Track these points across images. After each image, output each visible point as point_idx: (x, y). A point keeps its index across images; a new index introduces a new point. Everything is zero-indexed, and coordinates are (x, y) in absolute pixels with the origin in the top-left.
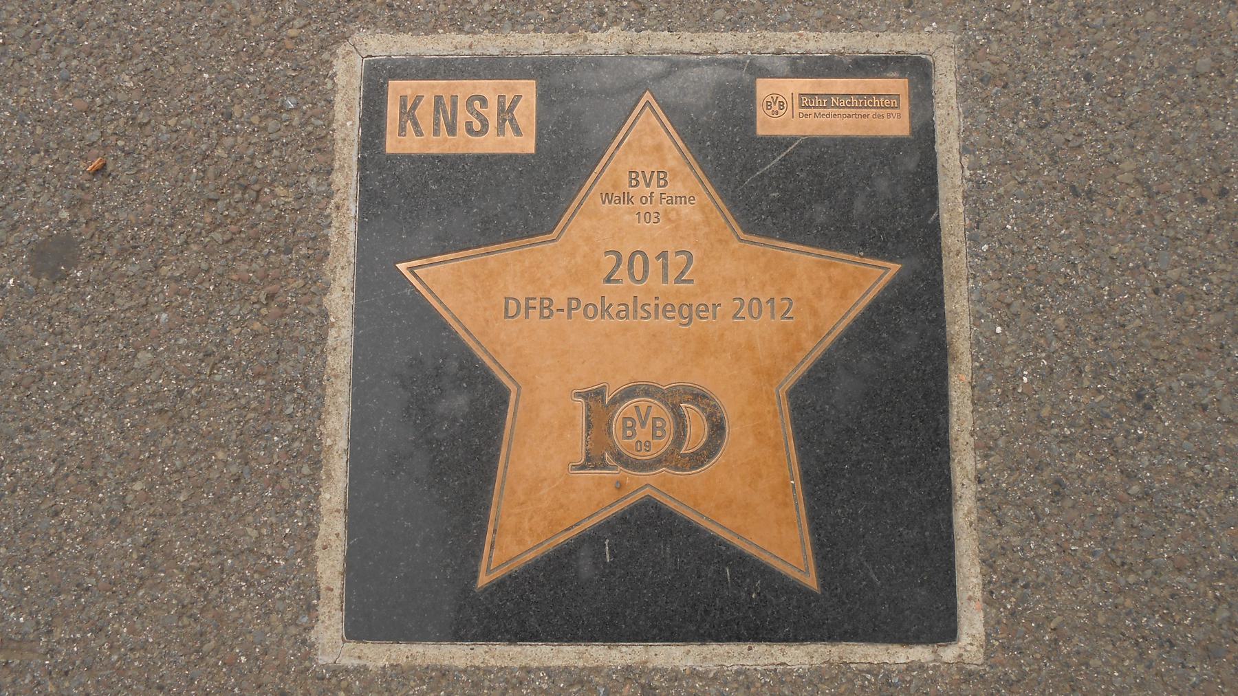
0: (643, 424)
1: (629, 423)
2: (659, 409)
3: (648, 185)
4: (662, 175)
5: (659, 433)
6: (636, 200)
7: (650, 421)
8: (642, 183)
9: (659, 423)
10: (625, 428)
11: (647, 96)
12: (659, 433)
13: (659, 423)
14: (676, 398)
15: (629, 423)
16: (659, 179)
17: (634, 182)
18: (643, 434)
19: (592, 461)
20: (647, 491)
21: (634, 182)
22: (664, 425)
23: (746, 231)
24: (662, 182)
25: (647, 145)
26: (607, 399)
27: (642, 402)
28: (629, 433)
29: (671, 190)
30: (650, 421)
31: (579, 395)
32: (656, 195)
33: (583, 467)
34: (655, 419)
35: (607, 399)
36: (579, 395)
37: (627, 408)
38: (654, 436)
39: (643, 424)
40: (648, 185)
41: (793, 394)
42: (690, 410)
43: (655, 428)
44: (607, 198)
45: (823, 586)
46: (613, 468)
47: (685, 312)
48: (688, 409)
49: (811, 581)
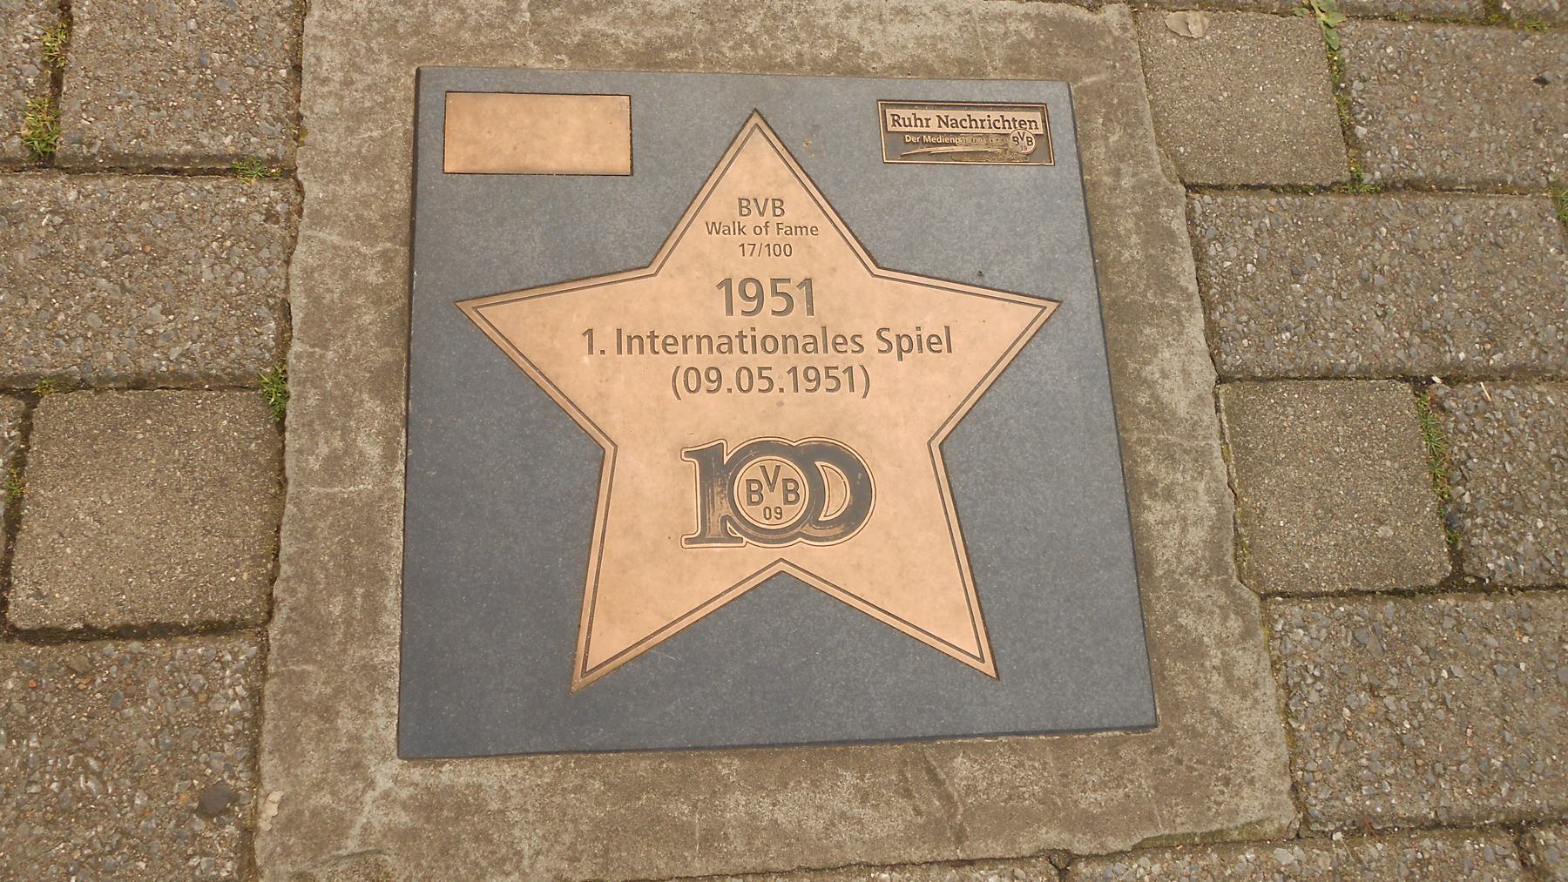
0: (772, 490)
1: (755, 487)
2: (791, 470)
3: (762, 214)
4: (778, 204)
5: (792, 497)
6: (749, 230)
7: (779, 480)
8: (755, 211)
9: (791, 486)
10: (750, 492)
12: (792, 497)
13: (791, 486)
14: (808, 455)
15: (755, 487)
17: (745, 211)
18: (774, 498)
20: (781, 566)
21: (745, 211)
24: (778, 212)
26: (726, 460)
27: (771, 461)
28: (755, 498)
29: (790, 218)
32: (772, 229)
33: (701, 539)
34: (786, 481)
35: (726, 460)
37: (751, 470)
38: (787, 502)
39: (772, 486)
40: (762, 214)
43: (787, 491)
44: (713, 228)
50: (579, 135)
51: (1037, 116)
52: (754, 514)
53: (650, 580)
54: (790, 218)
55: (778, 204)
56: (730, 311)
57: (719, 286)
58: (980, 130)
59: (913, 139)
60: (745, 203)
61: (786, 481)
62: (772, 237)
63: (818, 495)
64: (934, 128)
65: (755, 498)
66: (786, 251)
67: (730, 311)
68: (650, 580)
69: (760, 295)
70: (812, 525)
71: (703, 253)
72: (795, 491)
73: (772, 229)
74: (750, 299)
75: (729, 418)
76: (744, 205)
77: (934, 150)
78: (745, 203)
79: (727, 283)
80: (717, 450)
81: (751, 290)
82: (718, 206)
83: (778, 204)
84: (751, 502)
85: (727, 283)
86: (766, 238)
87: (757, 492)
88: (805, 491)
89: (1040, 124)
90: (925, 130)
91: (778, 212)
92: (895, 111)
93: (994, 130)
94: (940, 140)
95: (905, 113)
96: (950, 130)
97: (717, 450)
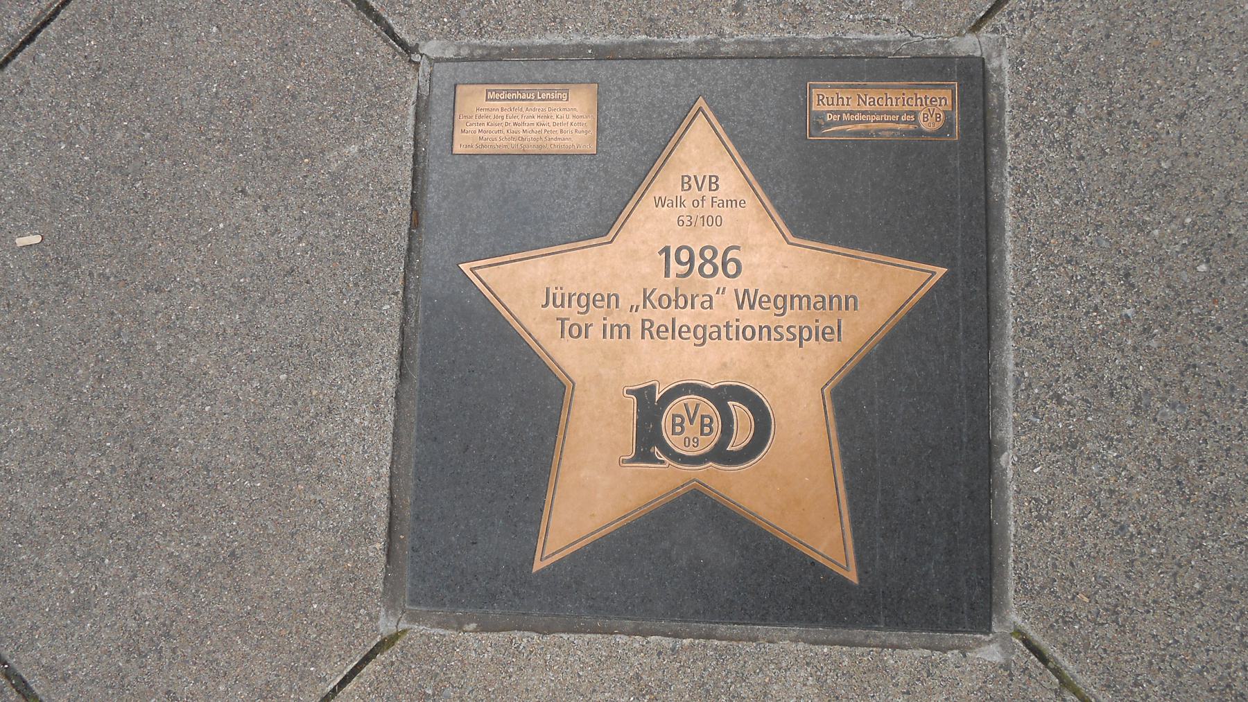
0: (691, 421)
1: (678, 420)
2: (708, 408)
3: (700, 189)
4: (714, 180)
5: (707, 430)
6: (688, 203)
11: (701, 102)
14: (721, 396)
16: (710, 182)
17: (686, 187)
18: (692, 430)
19: (643, 455)
21: (686, 187)
22: (712, 421)
23: (795, 234)
24: (714, 186)
25: (702, 149)
27: (691, 399)
28: (678, 429)
29: (721, 194)
30: (698, 419)
31: (629, 392)
32: (708, 203)
34: (703, 417)
35: (658, 397)
36: (629, 392)
39: (691, 421)
40: (700, 189)
41: (835, 393)
42: (738, 410)
43: (703, 425)
44: (660, 202)
45: (860, 579)
46: (662, 462)
47: (700, 332)
48: (736, 408)
49: (852, 576)
50: (562, 121)
51: (947, 94)
52: (675, 442)
53: (593, 490)
54: (721, 194)
55: (714, 180)
56: (667, 275)
57: (660, 253)
58: (895, 108)
59: (836, 118)
60: (686, 179)
61: (703, 417)
62: (707, 210)
63: (727, 430)
64: (853, 106)
65: (678, 429)
66: (716, 221)
67: (667, 275)
68: (593, 490)
69: (691, 260)
70: (720, 454)
71: (651, 223)
72: (710, 425)
73: (708, 203)
74: (686, 264)
75: (663, 364)
76: (686, 182)
77: (850, 128)
78: (686, 179)
79: (666, 250)
80: (652, 389)
81: (684, 256)
82: (666, 183)
83: (714, 182)
84: (674, 433)
85: (666, 250)
86: (699, 212)
87: (681, 425)
88: (717, 425)
89: (949, 102)
90: (843, 108)
91: (714, 186)
92: (820, 91)
93: (907, 108)
94: (858, 117)
95: (827, 93)
96: (867, 108)
97: (652, 389)
